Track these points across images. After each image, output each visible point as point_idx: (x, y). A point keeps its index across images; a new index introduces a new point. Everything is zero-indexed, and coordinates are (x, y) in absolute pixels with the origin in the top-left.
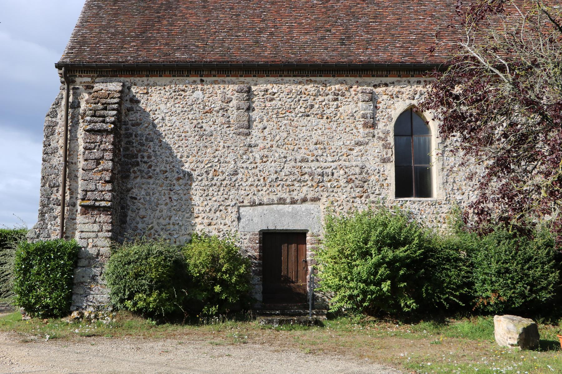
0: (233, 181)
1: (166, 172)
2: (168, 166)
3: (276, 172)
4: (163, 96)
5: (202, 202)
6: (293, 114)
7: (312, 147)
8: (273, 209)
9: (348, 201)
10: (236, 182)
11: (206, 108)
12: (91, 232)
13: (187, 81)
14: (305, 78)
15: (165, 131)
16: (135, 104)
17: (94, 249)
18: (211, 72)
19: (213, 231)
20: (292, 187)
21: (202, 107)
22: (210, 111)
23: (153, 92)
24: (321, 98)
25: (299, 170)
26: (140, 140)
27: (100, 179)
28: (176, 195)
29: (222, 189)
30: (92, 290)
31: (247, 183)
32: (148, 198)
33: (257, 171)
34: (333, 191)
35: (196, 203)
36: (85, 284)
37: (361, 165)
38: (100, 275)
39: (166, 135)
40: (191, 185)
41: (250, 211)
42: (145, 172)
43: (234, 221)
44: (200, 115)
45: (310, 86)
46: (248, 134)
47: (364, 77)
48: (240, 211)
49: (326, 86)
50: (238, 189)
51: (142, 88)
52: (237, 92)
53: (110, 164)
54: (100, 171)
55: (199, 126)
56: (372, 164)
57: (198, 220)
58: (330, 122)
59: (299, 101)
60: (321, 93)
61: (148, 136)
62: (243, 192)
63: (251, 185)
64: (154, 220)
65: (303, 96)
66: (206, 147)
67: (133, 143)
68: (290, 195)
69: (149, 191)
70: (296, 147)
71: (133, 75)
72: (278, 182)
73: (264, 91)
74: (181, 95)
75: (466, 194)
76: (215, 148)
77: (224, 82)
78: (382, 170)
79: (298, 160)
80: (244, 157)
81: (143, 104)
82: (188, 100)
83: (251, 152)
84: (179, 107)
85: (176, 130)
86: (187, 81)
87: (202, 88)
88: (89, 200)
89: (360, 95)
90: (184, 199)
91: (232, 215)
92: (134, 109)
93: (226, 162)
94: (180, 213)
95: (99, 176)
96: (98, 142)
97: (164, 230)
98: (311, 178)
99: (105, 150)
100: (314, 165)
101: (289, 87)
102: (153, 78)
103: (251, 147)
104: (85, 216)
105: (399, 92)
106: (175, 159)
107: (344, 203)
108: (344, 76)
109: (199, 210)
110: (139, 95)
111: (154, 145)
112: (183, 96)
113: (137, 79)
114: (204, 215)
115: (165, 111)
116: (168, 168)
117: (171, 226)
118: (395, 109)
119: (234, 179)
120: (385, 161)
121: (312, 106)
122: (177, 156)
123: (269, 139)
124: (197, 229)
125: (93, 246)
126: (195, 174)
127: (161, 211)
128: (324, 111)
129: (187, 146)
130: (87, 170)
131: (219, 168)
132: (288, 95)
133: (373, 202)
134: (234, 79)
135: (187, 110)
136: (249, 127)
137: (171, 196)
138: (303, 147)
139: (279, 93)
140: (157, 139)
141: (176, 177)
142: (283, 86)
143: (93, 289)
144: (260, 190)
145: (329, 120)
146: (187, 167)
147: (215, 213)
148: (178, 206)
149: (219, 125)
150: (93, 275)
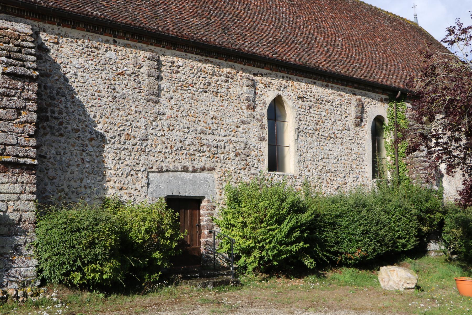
0: (144, 146)
1: (79, 131)
2: (80, 125)
3: (181, 141)
4: (75, 49)
5: (115, 166)
6: (195, 89)
7: (209, 121)
8: (177, 176)
9: (236, 172)
10: (147, 148)
11: (118, 70)
12: (11, 194)
13: (100, 39)
14: (204, 57)
15: (77, 87)
16: (44, 52)
17: (15, 213)
18: (125, 35)
19: (125, 196)
20: (193, 156)
21: (114, 68)
22: (122, 74)
23: (64, 43)
24: (215, 78)
25: (199, 141)
26: (50, 93)
27: (23, 132)
28: (89, 157)
29: (133, 153)
30: (15, 263)
31: (156, 149)
32: (58, 158)
33: (164, 138)
34: (224, 163)
35: (109, 166)
36: (5, 256)
37: (245, 141)
38: (24, 245)
39: (78, 92)
40: (103, 147)
41: (158, 177)
42: (56, 128)
43: (144, 186)
44: (113, 76)
45: (208, 65)
46: (157, 102)
47: (248, 65)
48: (149, 177)
49: (220, 68)
50: (148, 154)
51: (53, 36)
52: (148, 59)
53: (35, 116)
54: (22, 123)
55: (112, 87)
56: (253, 142)
57: (110, 184)
58: (223, 100)
59: (199, 77)
60: (216, 73)
61: (59, 90)
62: (152, 158)
63: (160, 152)
64: (65, 181)
65: (203, 73)
66: (119, 109)
67: (42, 95)
68: (192, 163)
69: (60, 150)
70: (197, 120)
71: (43, 20)
72: (182, 150)
73: (171, 63)
74: (94, 52)
75: (311, 171)
76: (127, 111)
77: (136, 47)
78: (259, 147)
79: (198, 132)
80: (154, 123)
81: (53, 54)
82: (100, 58)
83: (160, 120)
84: (92, 64)
85: (89, 88)
86: (100, 39)
87: (115, 49)
88: (8, 155)
89: (244, 81)
90: (96, 161)
91: (142, 180)
92: (43, 58)
93: (137, 127)
94: (92, 175)
95: (22, 129)
96: (19, 89)
97: (75, 194)
98: (208, 149)
99: (28, 99)
100: (211, 137)
101: (192, 63)
102: (65, 28)
103: (160, 114)
104: (4, 174)
105: (270, 83)
106: (87, 119)
107: (233, 174)
108: (233, 62)
109: (111, 174)
110: (48, 43)
111: (66, 100)
112: (96, 53)
113: (47, 26)
114: (116, 179)
115: (77, 66)
116: (81, 127)
117: (83, 189)
118: (268, 96)
119: (144, 145)
120: (262, 139)
121: (209, 84)
122: (90, 115)
123: (175, 109)
124: (109, 193)
125: (14, 210)
126: (108, 136)
127: (72, 173)
128: (218, 89)
129: (100, 106)
130: (5, 120)
131: (131, 133)
132: (191, 70)
133: (253, 174)
134: (144, 45)
135: (100, 68)
136: (158, 96)
137: (83, 157)
138: (202, 120)
139: (183, 67)
140: (70, 95)
141: (88, 137)
142: (187, 61)
143: (16, 262)
144: (167, 157)
145: (222, 98)
146: (100, 128)
147: (126, 177)
148: (90, 168)
149: (131, 89)
150: (15, 245)
